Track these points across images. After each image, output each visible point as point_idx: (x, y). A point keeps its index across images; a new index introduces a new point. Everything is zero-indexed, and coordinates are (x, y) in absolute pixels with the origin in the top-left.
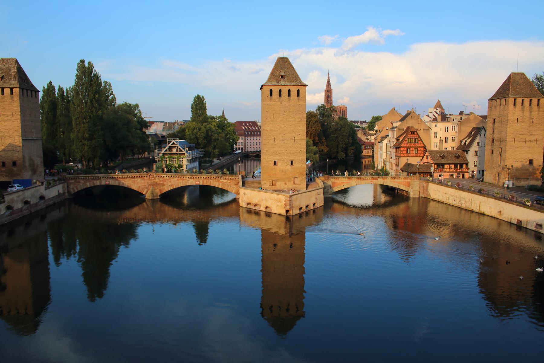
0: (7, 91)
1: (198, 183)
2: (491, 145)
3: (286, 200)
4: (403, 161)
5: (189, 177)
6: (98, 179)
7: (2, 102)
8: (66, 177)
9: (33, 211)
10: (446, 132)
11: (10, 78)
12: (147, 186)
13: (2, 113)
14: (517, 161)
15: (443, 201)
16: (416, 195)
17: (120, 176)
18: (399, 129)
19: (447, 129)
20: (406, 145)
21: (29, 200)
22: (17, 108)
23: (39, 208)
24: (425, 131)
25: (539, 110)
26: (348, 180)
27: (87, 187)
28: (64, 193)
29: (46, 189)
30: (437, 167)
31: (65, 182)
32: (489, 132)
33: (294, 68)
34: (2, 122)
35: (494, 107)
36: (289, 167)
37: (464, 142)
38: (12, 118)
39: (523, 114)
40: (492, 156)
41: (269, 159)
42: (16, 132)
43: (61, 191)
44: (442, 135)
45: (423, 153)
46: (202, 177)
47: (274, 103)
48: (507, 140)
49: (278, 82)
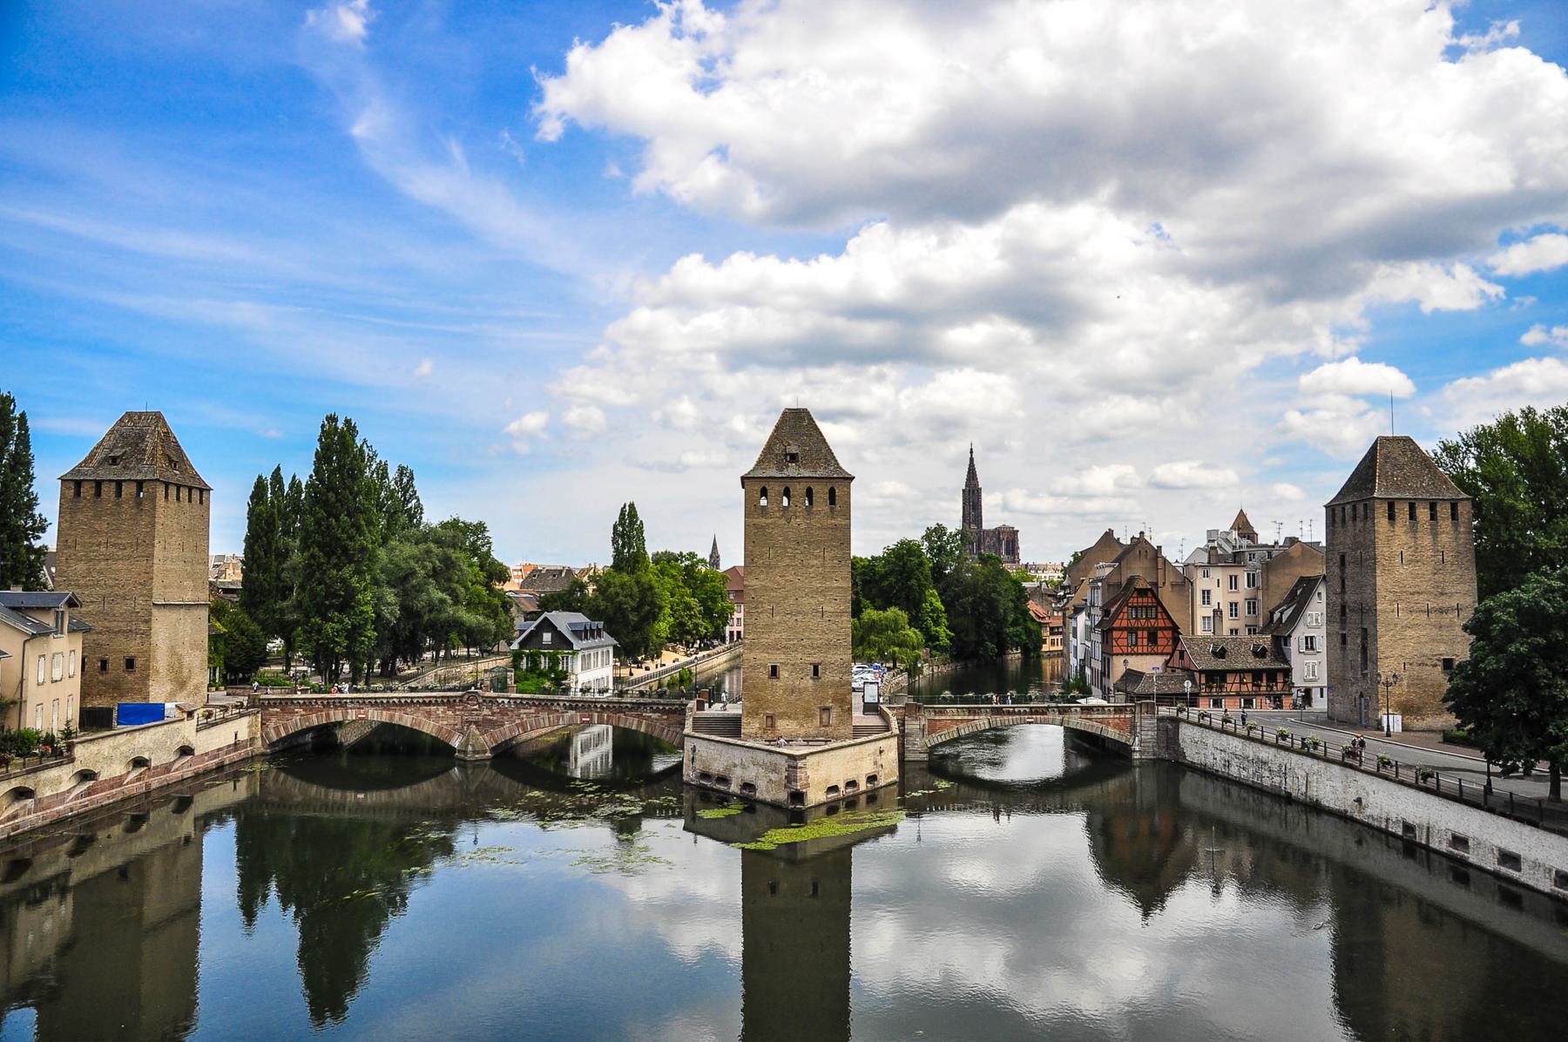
1: (588, 719)
2: (1339, 620)
3: (790, 767)
4: (1119, 667)
5: (564, 705)
6: (341, 706)
8: (260, 700)
9: (153, 787)
10: (1231, 588)
14: (1411, 664)
15: (1217, 771)
16: (1148, 753)
17: (395, 700)
18: (1109, 585)
19: (1233, 582)
20: (1124, 624)
21: (146, 757)
22: (149, 530)
23: (174, 775)
24: (1177, 588)
25: (1456, 530)
26: (969, 714)
27: (312, 725)
28: (252, 740)
29: (197, 731)
30: (1206, 680)
31: (258, 712)
32: (1332, 589)
33: (822, 436)
34: (109, 561)
35: (1340, 525)
36: (809, 682)
37: (1277, 616)
39: (1415, 542)
40: (1343, 649)
41: (758, 662)
42: (140, 587)
43: (244, 736)
44: (1221, 597)
45: (1170, 643)
46: (599, 706)
47: (770, 521)
48: (1378, 607)
49: (781, 470)
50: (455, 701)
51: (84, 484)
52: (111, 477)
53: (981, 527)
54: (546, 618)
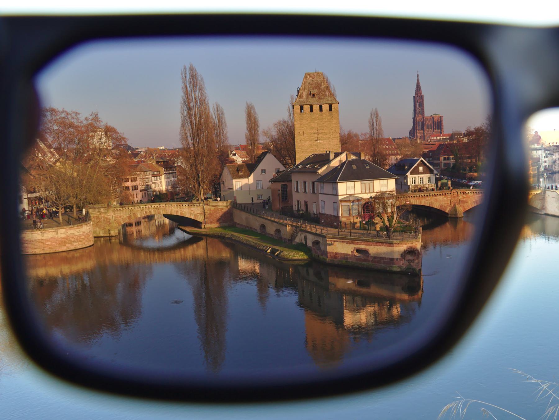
0: (326, 107)
7: (320, 120)
11: (323, 93)
12: (450, 204)
13: (320, 131)
17: (422, 195)
22: (336, 125)
38: (331, 136)
50: (448, 194)
51: (304, 106)
52: (316, 103)
53: (424, 115)
54: (422, 161)
